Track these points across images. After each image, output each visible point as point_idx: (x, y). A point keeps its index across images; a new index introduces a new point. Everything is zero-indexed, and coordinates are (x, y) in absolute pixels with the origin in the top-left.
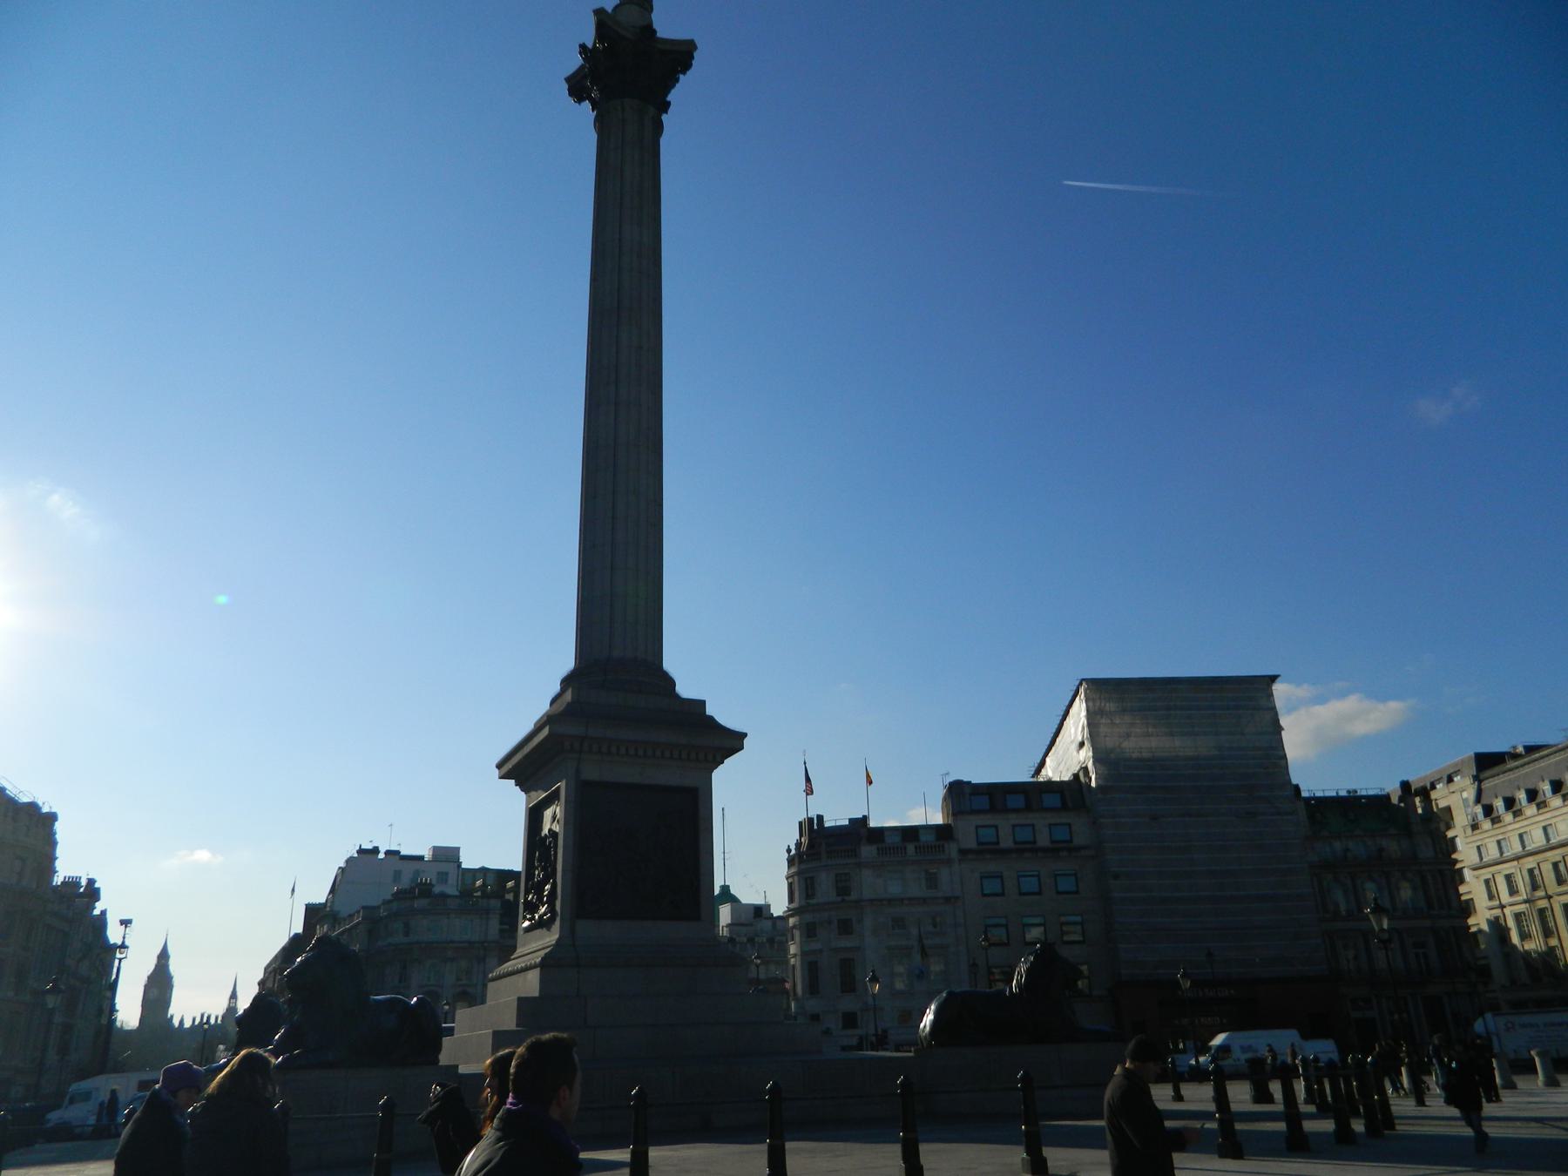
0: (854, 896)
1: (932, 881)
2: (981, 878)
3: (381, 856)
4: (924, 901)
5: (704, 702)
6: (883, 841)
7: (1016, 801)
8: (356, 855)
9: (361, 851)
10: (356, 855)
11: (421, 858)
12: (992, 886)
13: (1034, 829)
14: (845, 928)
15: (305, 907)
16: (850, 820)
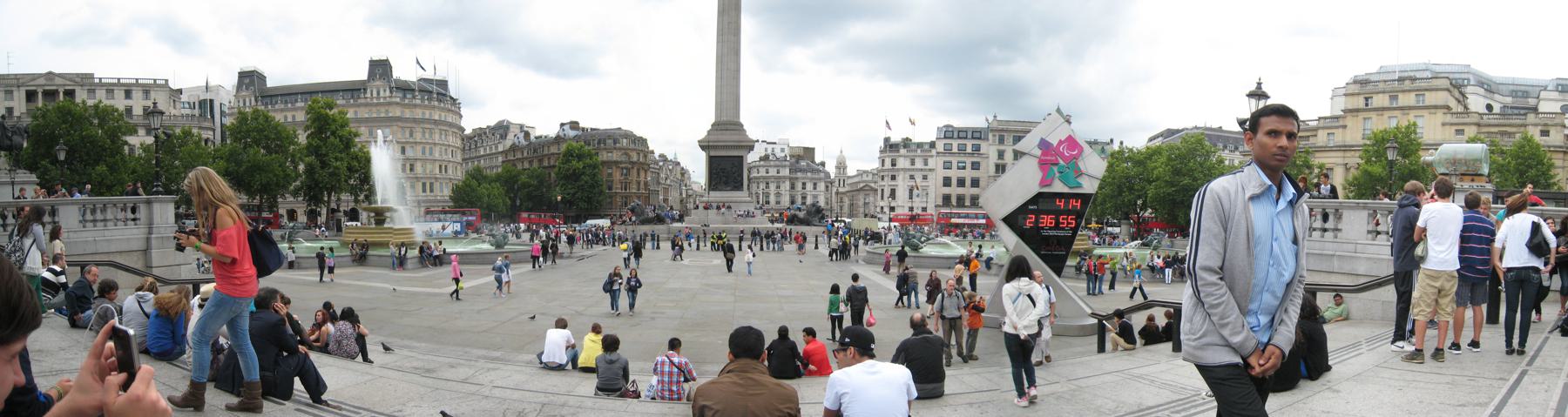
11: (775, 143)
14: (893, 178)
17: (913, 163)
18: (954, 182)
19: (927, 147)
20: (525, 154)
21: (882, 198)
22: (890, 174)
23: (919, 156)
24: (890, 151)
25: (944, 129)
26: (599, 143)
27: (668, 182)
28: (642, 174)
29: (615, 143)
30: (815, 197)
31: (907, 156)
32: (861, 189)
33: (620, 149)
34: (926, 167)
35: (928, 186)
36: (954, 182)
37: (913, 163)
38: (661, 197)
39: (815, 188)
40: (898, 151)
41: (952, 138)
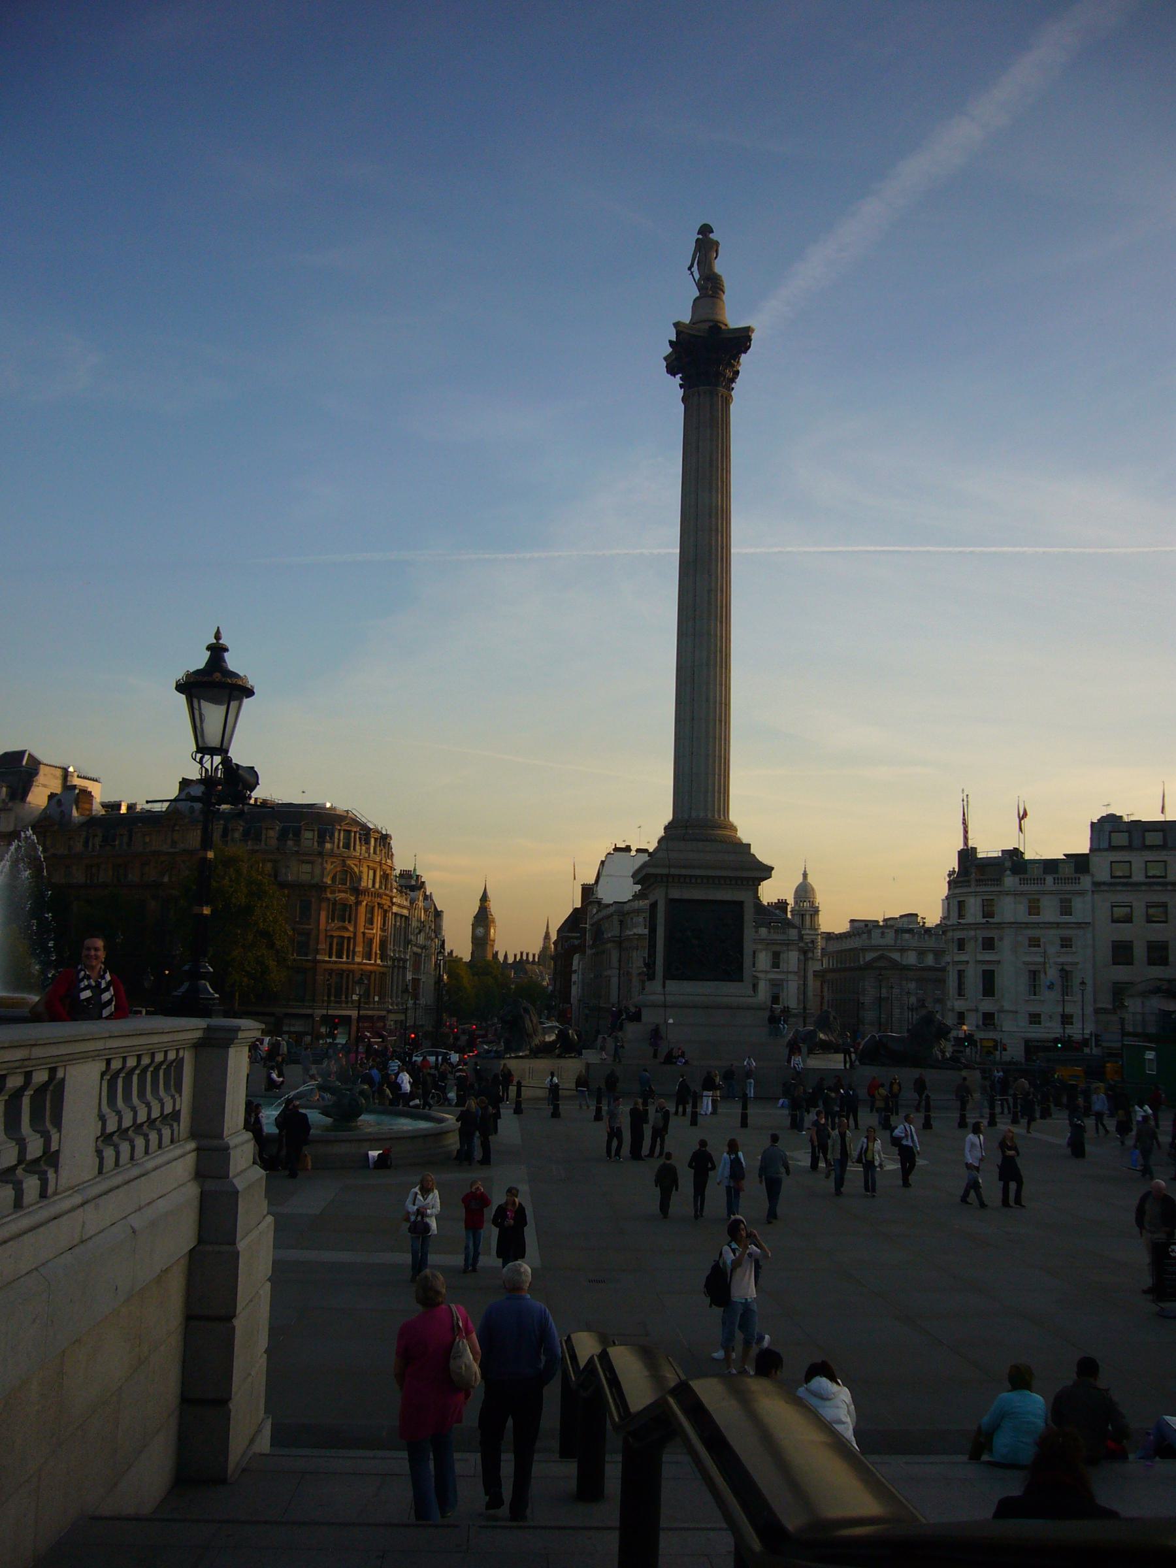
0: (996, 920)
1: (1066, 909)
2: (1112, 906)
3: (633, 853)
4: (1058, 925)
5: (750, 844)
6: (1025, 872)
7: (1153, 838)
8: (612, 852)
9: (617, 849)
10: (612, 852)
12: (1120, 912)
13: (1166, 866)
14: (989, 944)
15: (581, 887)
16: (1003, 851)
17: (1034, 909)
18: (1140, 952)
19: (1068, 871)
20: (79, 847)
21: (961, 993)
22: (981, 934)
23: (1051, 893)
24: (979, 882)
25: (1108, 827)
26: (283, 836)
27: (421, 939)
28: (378, 921)
29: (321, 842)
30: (776, 985)
31: (1022, 894)
32: (869, 966)
33: (332, 854)
34: (1067, 918)
35: (1077, 964)
36: (1140, 952)
37: (1034, 909)
38: (409, 976)
39: (776, 965)
40: (998, 881)
41: (1129, 848)
